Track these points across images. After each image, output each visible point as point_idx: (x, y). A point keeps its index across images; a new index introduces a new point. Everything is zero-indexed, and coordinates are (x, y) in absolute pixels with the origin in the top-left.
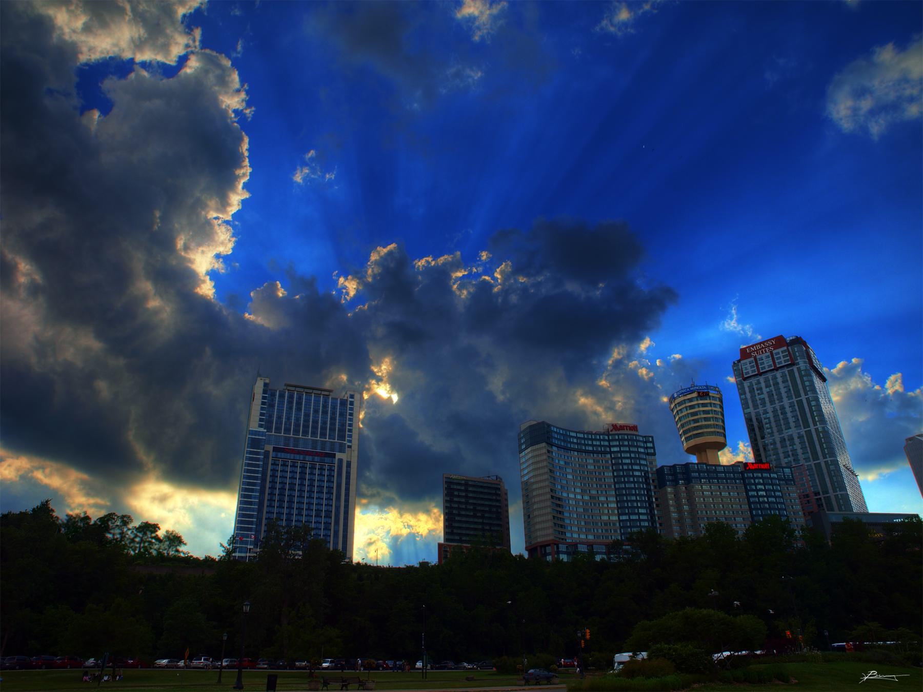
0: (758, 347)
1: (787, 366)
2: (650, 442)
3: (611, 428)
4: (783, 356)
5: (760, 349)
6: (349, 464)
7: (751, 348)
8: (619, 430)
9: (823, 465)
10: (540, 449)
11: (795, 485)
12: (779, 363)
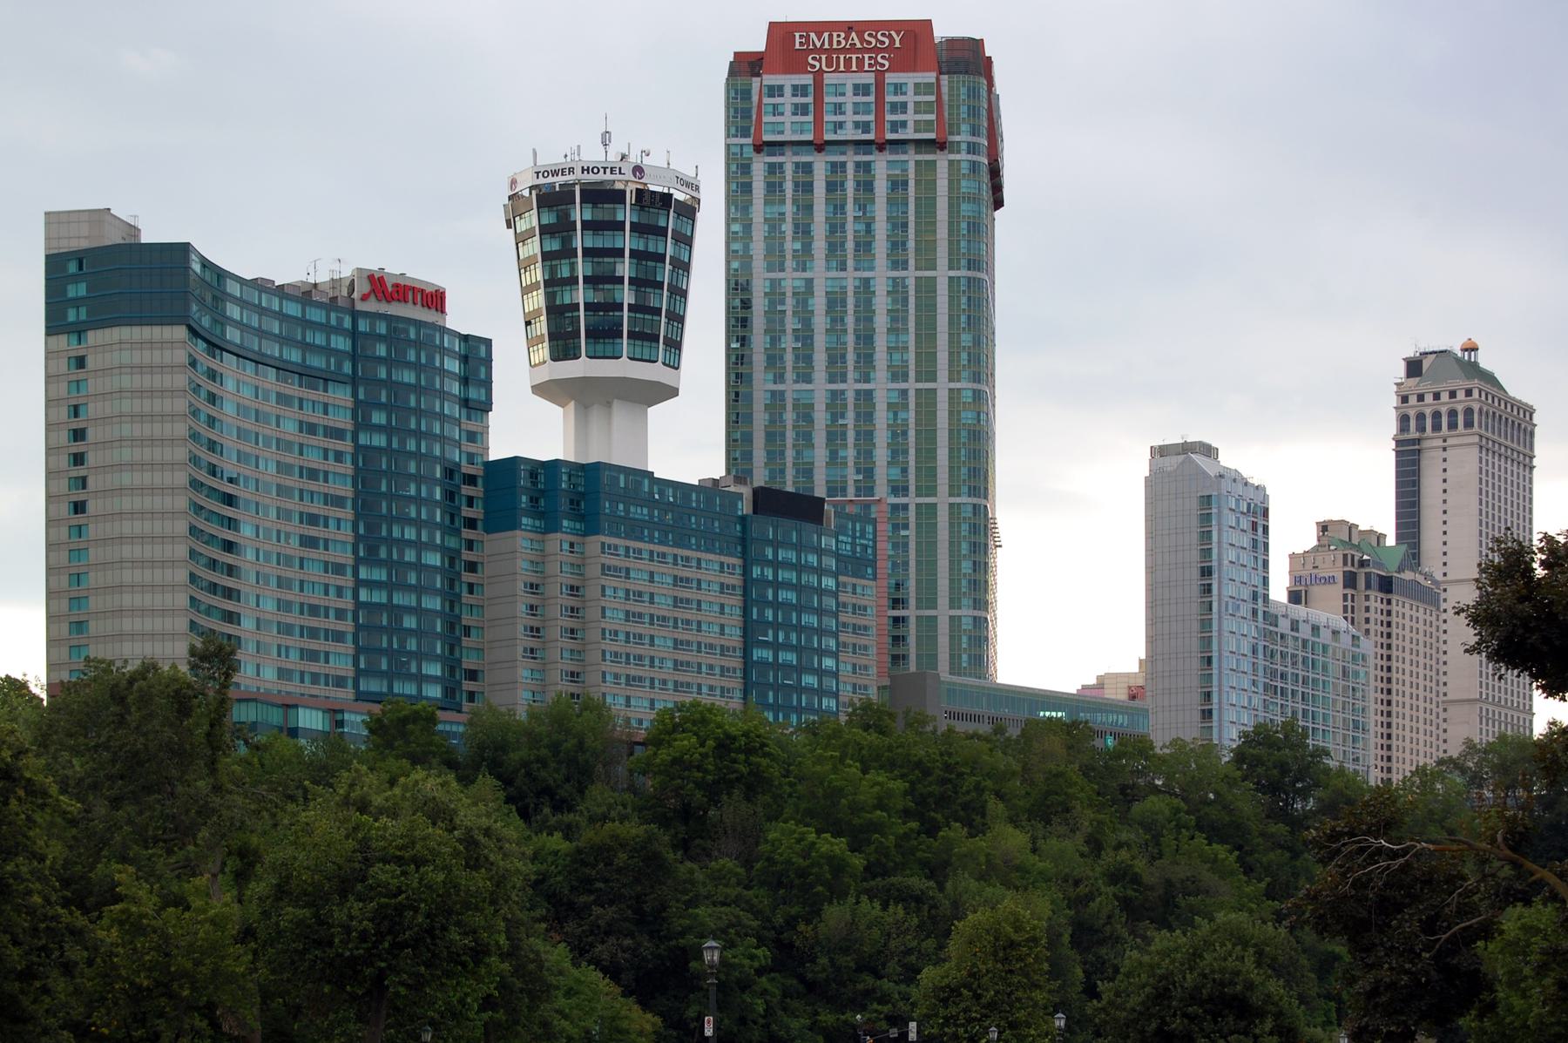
0: (839, 39)
1: (918, 143)
3: (362, 287)
5: (844, 50)
7: (813, 35)
8: (389, 298)
10: (163, 344)
11: (875, 579)
12: (895, 126)
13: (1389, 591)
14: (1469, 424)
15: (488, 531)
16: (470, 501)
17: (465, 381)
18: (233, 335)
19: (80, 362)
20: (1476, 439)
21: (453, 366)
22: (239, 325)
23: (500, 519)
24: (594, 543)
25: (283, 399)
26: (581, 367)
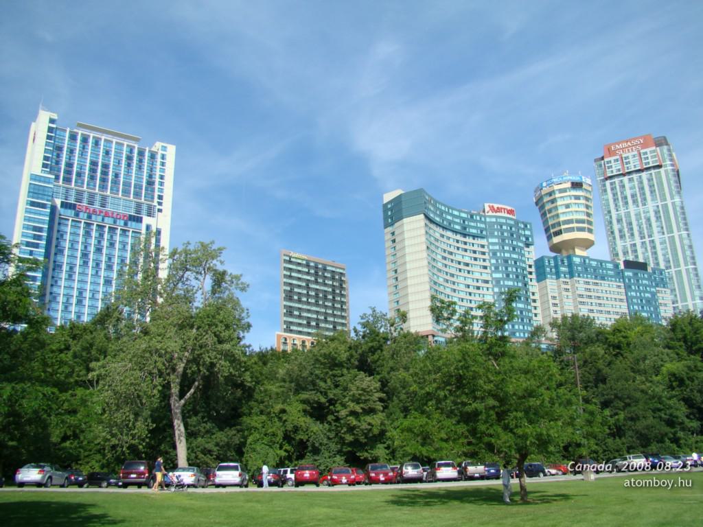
1: (655, 167)
2: (528, 230)
4: (652, 156)
6: (159, 232)
8: (496, 212)
12: (646, 164)
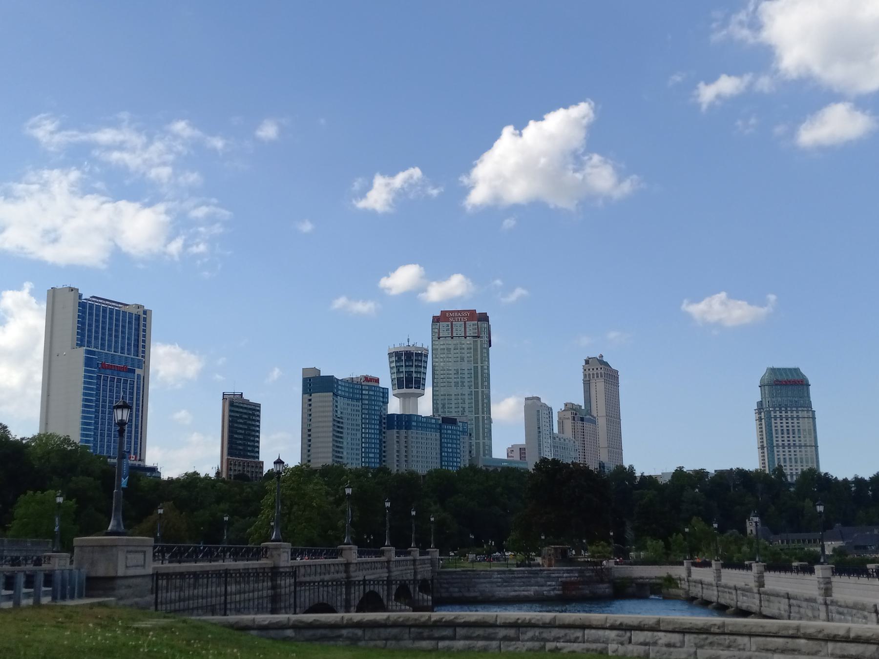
3: (363, 379)
5: (457, 317)
9: (481, 419)
13: (583, 421)
14: (601, 376)
15: (388, 429)
16: (384, 423)
17: (383, 397)
18: (340, 392)
19: (310, 400)
20: (603, 380)
21: (381, 394)
22: (341, 390)
23: (390, 427)
24: (410, 432)
25: (348, 404)
26: (404, 390)
